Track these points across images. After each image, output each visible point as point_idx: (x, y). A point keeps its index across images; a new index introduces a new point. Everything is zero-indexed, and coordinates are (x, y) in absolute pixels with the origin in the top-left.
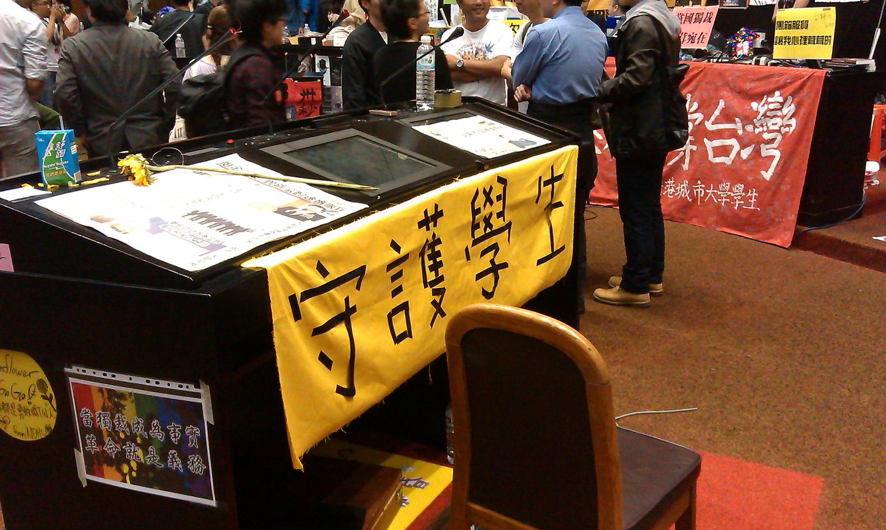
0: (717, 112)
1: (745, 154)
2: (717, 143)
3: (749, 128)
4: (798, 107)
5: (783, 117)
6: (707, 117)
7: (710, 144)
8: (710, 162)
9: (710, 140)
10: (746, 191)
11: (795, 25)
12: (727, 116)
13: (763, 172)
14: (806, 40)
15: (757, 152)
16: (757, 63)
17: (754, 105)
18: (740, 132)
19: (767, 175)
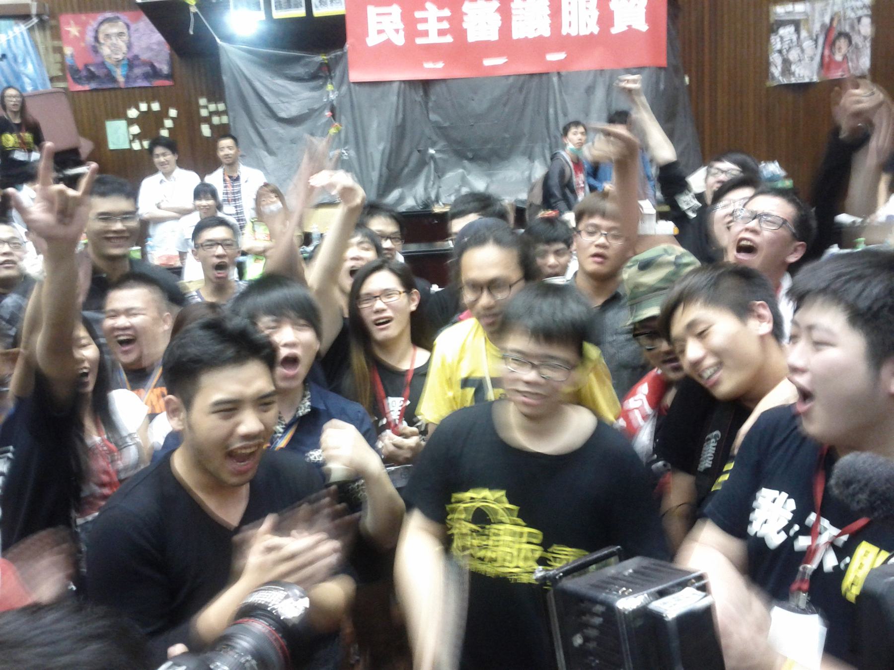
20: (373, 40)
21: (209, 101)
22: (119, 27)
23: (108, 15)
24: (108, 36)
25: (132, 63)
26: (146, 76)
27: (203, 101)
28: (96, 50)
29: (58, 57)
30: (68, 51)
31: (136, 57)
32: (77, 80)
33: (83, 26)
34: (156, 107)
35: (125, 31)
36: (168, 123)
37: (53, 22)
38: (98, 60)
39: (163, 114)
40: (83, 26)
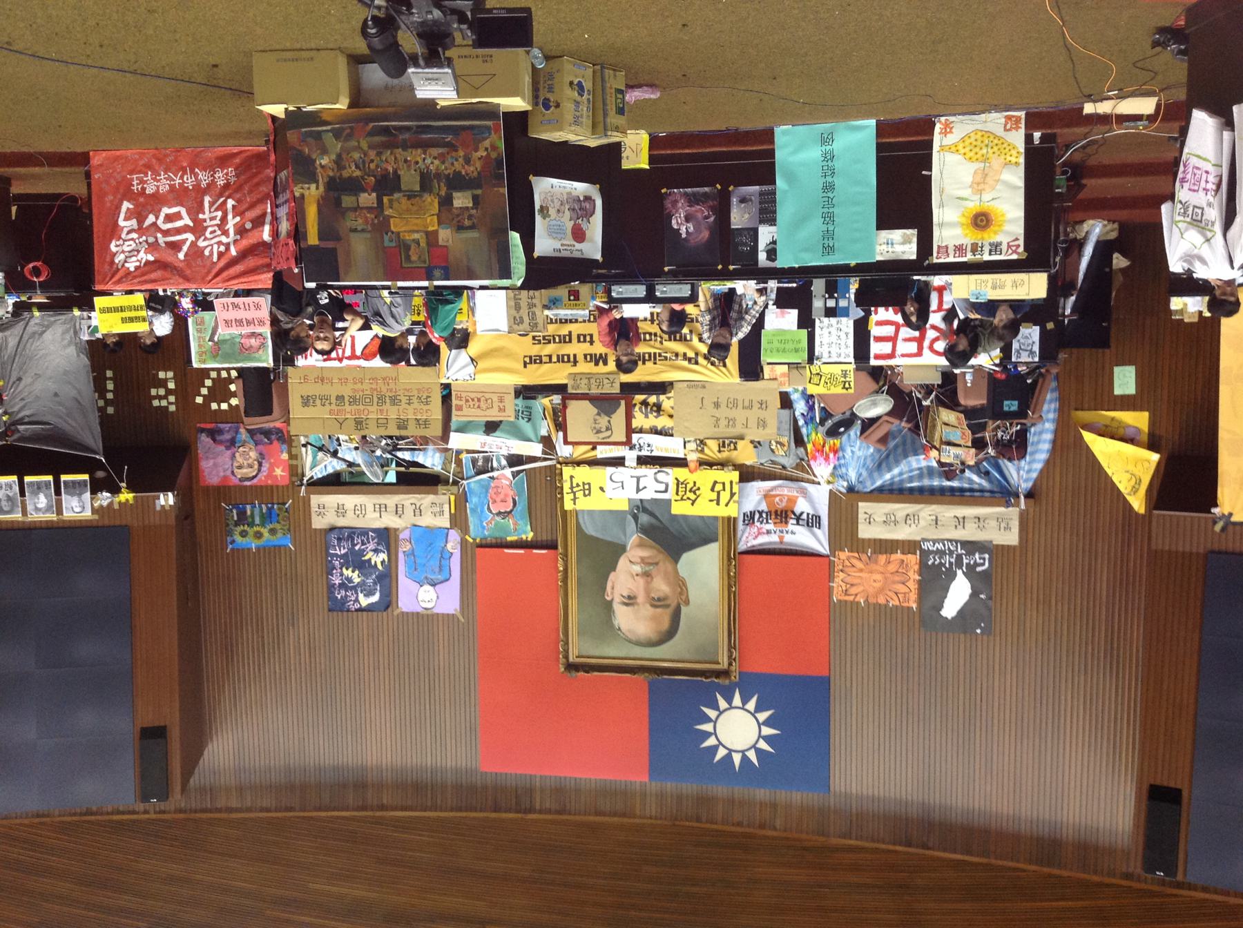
0: (185, 248)
1: (151, 219)
2: (179, 224)
3: (151, 240)
4: (112, 262)
5: (123, 252)
6: (193, 244)
7: (187, 221)
8: (182, 205)
9: (187, 226)
10: (144, 189)
11: (131, 320)
12: (176, 246)
13: (131, 207)
14: (122, 309)
15: (140, 222)
16: (165, 291)
17: (151, 258)
18: (159, 235)
19: (126, 205)
21: (167, 408)
22: (240, 473)
23: (248, 483)
24: (251, 466)
25: (232, 443)
26: (220, 432)
27: (172, 408)
29: (294, 451)
30: (285, 456)
31: (228, 448)
32: (279, 431)
34: (214, 406)
35: (236, 470)
36: (204, 391)
37: (294, 479)
38: (260, 447)
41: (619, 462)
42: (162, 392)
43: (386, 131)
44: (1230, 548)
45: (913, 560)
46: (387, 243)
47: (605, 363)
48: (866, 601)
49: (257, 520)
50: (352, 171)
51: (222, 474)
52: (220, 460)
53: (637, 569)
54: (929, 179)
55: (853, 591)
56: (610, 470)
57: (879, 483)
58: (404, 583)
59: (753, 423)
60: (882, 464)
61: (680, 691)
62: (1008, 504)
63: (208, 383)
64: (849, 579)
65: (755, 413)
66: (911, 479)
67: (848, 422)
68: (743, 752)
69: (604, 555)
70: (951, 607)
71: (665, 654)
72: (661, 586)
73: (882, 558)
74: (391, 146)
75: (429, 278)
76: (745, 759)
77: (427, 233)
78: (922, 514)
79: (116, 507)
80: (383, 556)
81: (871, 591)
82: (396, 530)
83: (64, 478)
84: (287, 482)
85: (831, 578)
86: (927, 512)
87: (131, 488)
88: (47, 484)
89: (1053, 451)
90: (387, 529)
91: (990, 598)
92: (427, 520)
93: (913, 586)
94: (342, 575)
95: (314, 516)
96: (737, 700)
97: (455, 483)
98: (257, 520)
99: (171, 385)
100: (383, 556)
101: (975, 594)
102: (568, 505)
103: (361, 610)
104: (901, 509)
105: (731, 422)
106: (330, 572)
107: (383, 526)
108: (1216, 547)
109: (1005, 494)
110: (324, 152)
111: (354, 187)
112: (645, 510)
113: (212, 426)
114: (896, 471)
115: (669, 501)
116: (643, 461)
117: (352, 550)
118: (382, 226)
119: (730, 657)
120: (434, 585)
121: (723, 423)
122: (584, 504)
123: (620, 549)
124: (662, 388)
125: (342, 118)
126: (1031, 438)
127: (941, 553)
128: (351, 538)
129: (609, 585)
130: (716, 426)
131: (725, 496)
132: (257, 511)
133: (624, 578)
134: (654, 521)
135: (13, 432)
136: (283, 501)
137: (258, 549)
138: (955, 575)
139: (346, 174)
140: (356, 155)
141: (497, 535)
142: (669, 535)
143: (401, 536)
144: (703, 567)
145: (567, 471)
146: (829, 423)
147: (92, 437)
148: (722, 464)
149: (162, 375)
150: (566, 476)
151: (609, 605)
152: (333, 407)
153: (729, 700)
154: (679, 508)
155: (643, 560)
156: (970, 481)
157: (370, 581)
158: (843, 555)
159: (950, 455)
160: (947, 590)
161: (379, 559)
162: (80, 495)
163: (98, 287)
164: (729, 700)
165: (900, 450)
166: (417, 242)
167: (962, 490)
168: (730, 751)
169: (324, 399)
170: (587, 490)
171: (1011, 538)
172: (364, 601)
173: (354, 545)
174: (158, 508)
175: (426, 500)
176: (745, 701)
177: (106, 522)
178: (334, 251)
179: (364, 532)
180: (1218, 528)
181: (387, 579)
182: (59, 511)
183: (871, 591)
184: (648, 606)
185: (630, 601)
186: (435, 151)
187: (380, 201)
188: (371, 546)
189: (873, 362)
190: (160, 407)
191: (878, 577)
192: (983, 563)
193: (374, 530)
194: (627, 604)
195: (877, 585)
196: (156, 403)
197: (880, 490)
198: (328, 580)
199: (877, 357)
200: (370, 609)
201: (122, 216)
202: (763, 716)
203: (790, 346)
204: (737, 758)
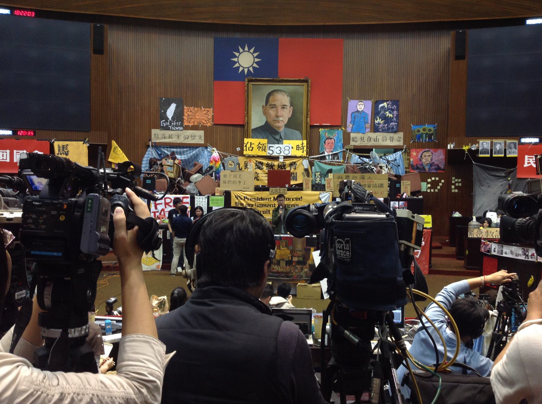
19: (418, 256)
20: (526, 165)
22: (430, 153)
23: (427, 150)
25: (431, 165)
26: (436, 169)
27: (453, 178)
28: (421, 160)
29: (408, 162)
30: (412, 160)
31: (433, 163)
32: (413, 169)
33: (418, 152)
34: (437, 179)
36: (441, 184)
38: (421, 163)
39: (439, 181)
40: (418, 152)
41: (285, 157)
42: (457, 184)
43: (288, 277)
44: (83, 133)
45: (186, 123)
46: (291, 247)
47: (274, 198)
48: (201, 108)
49: (424, 135)
50: (299, 267)
51: (437, 153)
52: (437, 158)
53: (281, 119)
54: (163, 253)
55: (205, 112)
56: (289, 155)
57: (197, 150)
58: (369, 112)
59: (228, 176)
60: (196, 157)
61: (267, 72)
62: (155, 143)
63: (439, 187)
64: (207, 116)
65: (227, 180)
66: (187, 151)
67: (207, 171)
68: (244, 51)
69: (293, 124)
70: (173, 107)
71: (271, 87)
72: (272, 112)
73: (196, 124)
74: (287, 273)
75: (281, 237)
76: (243, 49)
77: (280, 249)
78: (183, 139)
79: (470, 144)
80: (376, 122)
81: (200, 112)
82: (371, 132)
83: (489, 156)
84: (412, 150)
85: (213, 116)
86: (181, 140)
87: (464, 151)
88: (495, 153)
89: (141, 161)
90: (375, 132)
91: (161, 111)
92: (359, 135)
93: (186, 114)
94: (393, 115)
95: (402, 137)
96: (246, 70)
97: (347, 150)
98: (424, 135)
99: (453, 187)
100: (376, 122)
101: (165, 112)
102: (305, 142)
103: (386, 101)
104: (190, 141)
105: (235, 176)
106: (398, 115)
107: (376, 133)
108: (87, 133)
109: (157, 146)
110: (306, 272)
111: (298, 263)
112: (277, 140)
113: (438, 171)
114: (191, 154)
115: (268, 143)
116: (277, 158)
117: (389, 124)
118: (292, 252)
119: (248, 87)
120: (358, 111)
121: (238, 176)
122: (299, 142)
123: (287, 126)
124: (257, 189)
125: (300, 281)
126: (148, 165)
127: (176, 126)
128: (388, 129)
129: (291, 113)
130: (240, 175)
131: (248, 145)
132: (424, 139)
133: (286, 115)
134: (274, 136)
135: (506, 173)
136: (414, 142)
137: (425, 125)
138: (172, 118)
139: (301, 266)
140: (297, 271)
141: (333, 131)
142: (269, 132)
143: (369, 129)
144: (257, 120)
145: (305, 154)
146: (211, 172)
147: (477, 171)
148: (249, 157)
149: (456, 191)
150: (305, 152)
151: (292, 104)
152: (372, 183)
153: (249, 70)
154: (265, 141)
155: (279, 122)
156: (167, 151)
157: (382, 112)
158: (209, 125)
159: (170, 162)
160: (174, 113)
161: (378, 121)
162: (483, 149)
163: (430, 230)
164: (249, 70)
165: (191, 161)
166: (283, 247)
167: (170, 147)
168: (249, 51)
169: (375, 186)
170: (298, 148)
171: (154, 131)
172: (385, 104)
173: (387, 126)
174: (454, 143)
175: (358, 143)
176: (243, 70)
177: (474, 138)
178: (307, 245)
179: (383, 131)
180: (87, 139)
181: (376, 113)
182: (492, 143)
183: (200, 112)
184: (277, 105)
185: (284, 107)
186: (275, 271)
187: (292, 258)
188: (381, 126)
189: (189, 196)
190: (458, 179)
191: (197, 117)
192: (163, 123)
193: (380, 132)
194: (285, 105)
195: (198, 114)
196: (460, 180)
197: (197, 148)
198: (398, 112)
199: (188, 197)
200: (383, 102)
201: (419, 253)
202: (237, 65)
203: (215, 201)
204: (246, 49)
